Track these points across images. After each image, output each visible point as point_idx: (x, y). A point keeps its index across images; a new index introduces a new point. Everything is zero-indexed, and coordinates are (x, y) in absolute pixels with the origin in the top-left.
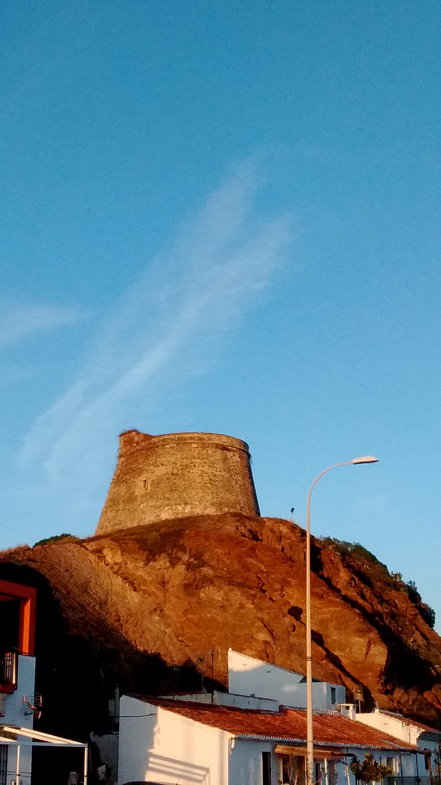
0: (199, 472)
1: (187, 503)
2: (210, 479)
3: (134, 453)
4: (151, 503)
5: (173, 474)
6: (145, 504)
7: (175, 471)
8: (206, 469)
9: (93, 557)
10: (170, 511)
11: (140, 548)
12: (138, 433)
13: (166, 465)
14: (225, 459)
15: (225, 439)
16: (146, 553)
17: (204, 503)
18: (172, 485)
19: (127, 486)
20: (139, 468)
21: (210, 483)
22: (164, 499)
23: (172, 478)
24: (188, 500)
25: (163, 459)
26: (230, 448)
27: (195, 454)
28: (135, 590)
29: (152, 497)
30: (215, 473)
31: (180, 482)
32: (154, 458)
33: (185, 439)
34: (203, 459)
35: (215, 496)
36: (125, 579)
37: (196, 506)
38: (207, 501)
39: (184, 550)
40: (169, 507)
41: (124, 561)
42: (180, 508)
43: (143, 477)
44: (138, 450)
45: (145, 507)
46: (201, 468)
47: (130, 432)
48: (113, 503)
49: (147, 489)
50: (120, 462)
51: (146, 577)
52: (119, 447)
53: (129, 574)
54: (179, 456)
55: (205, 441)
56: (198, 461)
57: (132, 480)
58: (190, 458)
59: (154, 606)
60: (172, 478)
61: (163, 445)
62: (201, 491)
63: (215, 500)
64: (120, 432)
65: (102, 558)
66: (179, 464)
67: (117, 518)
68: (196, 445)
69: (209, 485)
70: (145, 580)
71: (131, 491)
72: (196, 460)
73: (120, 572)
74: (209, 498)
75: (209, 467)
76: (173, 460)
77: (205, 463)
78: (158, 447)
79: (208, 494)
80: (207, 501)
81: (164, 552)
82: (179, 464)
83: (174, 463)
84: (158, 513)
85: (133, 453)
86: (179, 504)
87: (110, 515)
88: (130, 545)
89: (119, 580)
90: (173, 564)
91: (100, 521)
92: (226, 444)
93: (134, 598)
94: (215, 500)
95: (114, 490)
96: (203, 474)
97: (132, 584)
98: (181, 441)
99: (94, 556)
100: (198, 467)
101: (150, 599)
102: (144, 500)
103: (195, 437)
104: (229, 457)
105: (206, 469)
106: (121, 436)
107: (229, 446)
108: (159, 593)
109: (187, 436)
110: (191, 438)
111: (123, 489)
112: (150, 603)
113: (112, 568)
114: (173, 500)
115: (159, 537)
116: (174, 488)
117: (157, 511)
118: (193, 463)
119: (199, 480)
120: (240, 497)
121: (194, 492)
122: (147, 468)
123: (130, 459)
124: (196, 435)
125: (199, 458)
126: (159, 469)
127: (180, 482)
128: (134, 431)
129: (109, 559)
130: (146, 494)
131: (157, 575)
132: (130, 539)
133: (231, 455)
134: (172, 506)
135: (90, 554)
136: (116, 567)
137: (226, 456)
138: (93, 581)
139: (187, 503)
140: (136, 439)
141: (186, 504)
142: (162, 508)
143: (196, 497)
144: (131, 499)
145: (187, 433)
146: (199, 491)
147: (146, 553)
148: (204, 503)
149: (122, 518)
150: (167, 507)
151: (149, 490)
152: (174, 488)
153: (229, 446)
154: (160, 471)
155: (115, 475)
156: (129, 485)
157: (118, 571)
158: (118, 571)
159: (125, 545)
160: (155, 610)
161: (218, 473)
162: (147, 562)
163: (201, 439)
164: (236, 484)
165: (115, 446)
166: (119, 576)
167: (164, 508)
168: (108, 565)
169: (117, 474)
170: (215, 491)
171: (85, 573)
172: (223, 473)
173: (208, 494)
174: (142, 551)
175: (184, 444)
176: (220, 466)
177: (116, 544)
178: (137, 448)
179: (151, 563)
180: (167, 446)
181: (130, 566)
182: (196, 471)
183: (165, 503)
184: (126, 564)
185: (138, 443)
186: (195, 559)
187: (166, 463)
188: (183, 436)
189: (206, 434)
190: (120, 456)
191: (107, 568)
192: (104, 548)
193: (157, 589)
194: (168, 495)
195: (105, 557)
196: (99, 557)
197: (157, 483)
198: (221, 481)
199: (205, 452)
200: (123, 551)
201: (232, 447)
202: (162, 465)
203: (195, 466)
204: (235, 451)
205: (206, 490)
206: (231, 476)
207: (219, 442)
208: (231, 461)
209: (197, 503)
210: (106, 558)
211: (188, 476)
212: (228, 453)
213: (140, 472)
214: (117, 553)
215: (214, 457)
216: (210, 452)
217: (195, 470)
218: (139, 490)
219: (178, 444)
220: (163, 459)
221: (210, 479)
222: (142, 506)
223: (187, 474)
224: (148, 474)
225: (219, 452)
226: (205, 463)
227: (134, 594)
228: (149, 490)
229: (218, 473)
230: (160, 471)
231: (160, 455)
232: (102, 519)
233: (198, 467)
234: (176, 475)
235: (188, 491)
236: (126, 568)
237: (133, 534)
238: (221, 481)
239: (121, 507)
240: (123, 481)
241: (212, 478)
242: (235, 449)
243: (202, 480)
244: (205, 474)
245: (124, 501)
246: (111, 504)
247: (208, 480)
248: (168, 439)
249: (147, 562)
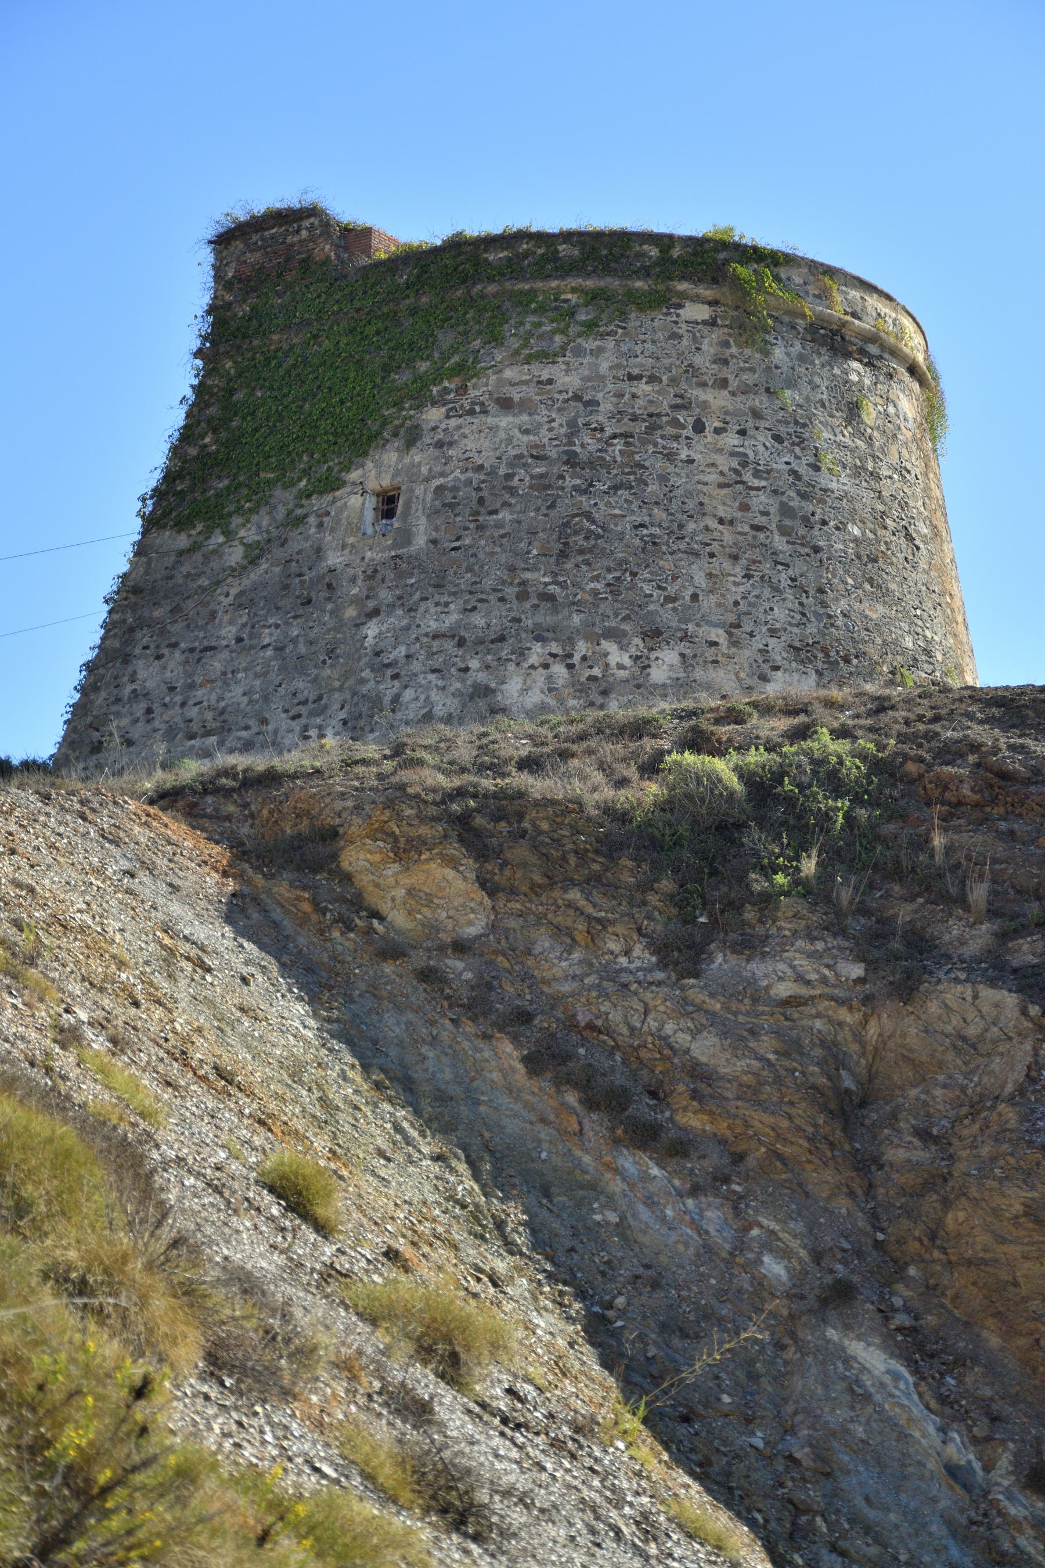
0: (725, 463)
2: (786, 511)
5: (571, 460)
6: (397, 619)
7: (588, 444)
8: (759, 445)
10: (559, 670)
13: (526, 406)
17: (757, 643)
21: (784, 531)
22: (522, 596)
23: (569, 482)
24: (667, 617)
27: (698, 360)
34: (745, 390)
37: (710, 653)
38: (773, 632)
40: (555, 648)
43: (380, 469)
46: (731, 440)
49: (405, 537)
51: (706, 1048)
54: (604, 367)
56: (717, 400)
58: (674, 381)
60: (569, 482)
66: (607, 406)
69: (779, 542)
70: (700, 1074)
74: (780, 615)
75: (778, 438)
79: (776, 589)
82: (607, 406)
83: (577, 397)
84: (482, 677)
86: (611, 634)
94: (812, 629)
96: (748, 476)
100: (718, 431)
105: (759, 445)
117: (474, 664)
118: (686, 407)
119: (722, 504)
125: (723, 383)
126: (492, 421)
134: (571, 641)
139: (657, 633)
141: (654, 635)
143: (707, 602)
146: (727, 565)
148: (757, 643)
149: (236, 694)
150: (537, 648)
151: (420, 541)
154: (486, 439)
165: (185, 295)
167: (522, 653)
173: (776, 589)
182: (709, 456)
187: (530, 391)
197: (473, 503)
202: (506, 404)
203: (699, 427)
205: (767, 567)
209: (718, 635)
211: (663, 478)
217: (698, 451)
221: (786, 511)
222: (372, 630)
223: (659, 465)
226: (757, 414)
228: (420, 541)
230: (486, 439)
233: (718, 431)
234: (591, 464)
235: (666, 564)
239: (228, 632)
241: (796, 503)
243: (745, 507)
244: (757, 474)
245: (244, 602)
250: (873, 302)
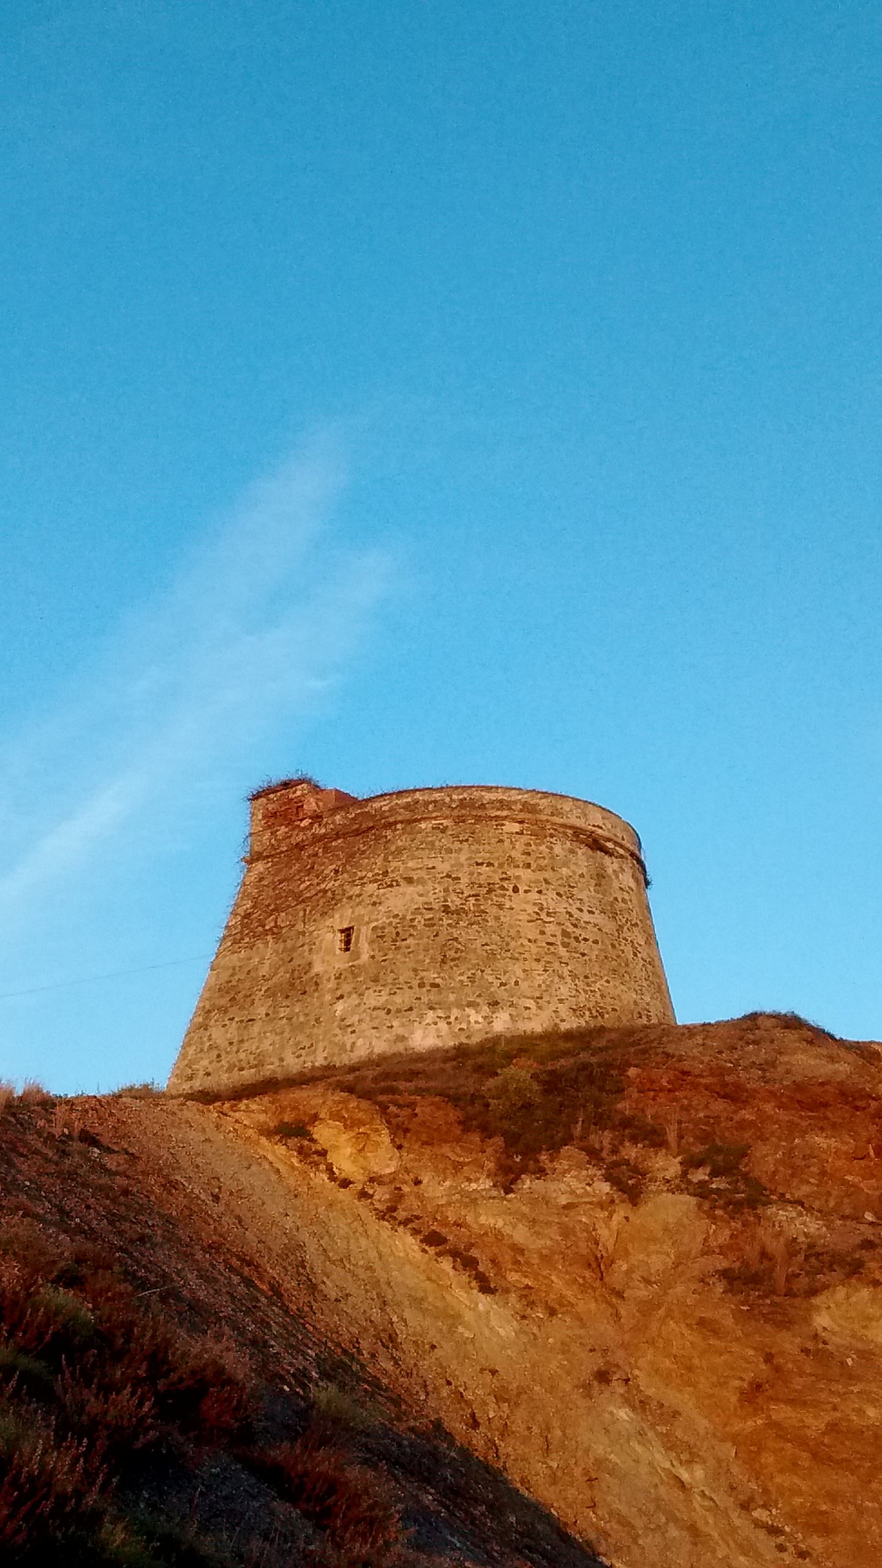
0: (531, 909)
1: (497, 1003)
2: (565, 934)
3: (302, 848)
4: (372, 999)
5: (446, 909)
6: (354, 1000)
7: (454, 901)
8: (550, 899)
9: (278, 1152)
10: (442, 1025)
11: (465, 1125)
12: (316, 789)
13: (421, 881)
14: (600, 877)
15: (596, 818)
16: (499, 1141)
18: (449, 940)
19: (281, 946)
20: (325, 891)
21: (565, 945)
22: (421, 985)
23: (446, 922)
24: (502, 994)
25: (410, 864)
26: (610, 845)
27: (513, 854)
28: (486, 1288)
29: (376, 980)
30: (576, 914)
31: (470, 935)
32: (379, 861)
33: (483, 806)
34: (541, 869)
35: (581, 984)
36: (433, 1239)
37: (526, 1013)
38: (561, 1001)
39: (655, 1139)
40: (440, 1013)
41: (407, 1171)
42: (474, 1016)
43: (340, 919)
44: (317, 839)
45: (353, 1013)
46: (534, 896)
47: (286, 785)
48: (226, 998)
50: (253, 877)
51: (520, 1234)
52: (247, 830)
53: (445, 1223)
54: (463, 858)
55: (544, 818)
56: (525, 874)
57: (300, 927)
58: (501, 865)
59: (590, 1363)
60: (446, 922)
61: (409, 822)
62: (540, 967)
63: (582, 998)
64: (257, 783)
65: (314, 1156)
66: (465, 880)
67: (246, 1045)
68: (516, 827)
69: (562, 951)
71: (295, 962)
72: (520, 872)
73: (401, 1214)
74: (564, 991)
75: (558, 894)
76: (444, 867)
77: (547, 882)
78: (390, 825)
79: (561, 977)
80: (561, 1001)
81: (568, 1140)
82: (465, 880)
83: (448, 876)
84: (401, 1031)
85: (300, 847)
86: (470, 1004)
87: (218, 1035)
88: (424, 1110)
89: (407, 1244)
90: (630, 1186)
91: (183, 1055)
92: (600, 831)
93: (490, 1324)
94: (582, 998)
95: (234, 959)
96: (543, 916)
97: (466, 1262)
98: (470, 810)
99: (281, 1149)
100: (526, 892)
101: (560, 1329)
102: (346, 988)
103: (515, 802)
104: (610, 871)
105: (550, 899)
106: (256, 797)
107: (609, 840)
108: (587, 1305)
109: (488, 796)
110: (502, 804)
111: (266, 956)
112: (564, 1348)
113: (363, 1195)
114: (453, 990)
115: (536, 1087)
116: (451, 954)
120: (648, 999)
121: (517, 969)
122: (357, 890)
123: (288, 865)
124: (515, 796)
125: (529, 866)
126: (404, 890)
127: (470, 935)
128: (301, 781)
129: (344, 1160)
130: (354, 971)
131: (566, 1232)
132: (419, 1091)
133: (616, 866)
134: (449, 1009)
135: (263, 1140)
136: (381, 1194)
137: (603, 867)
138: (312, 1247)
139: (497, 1003)
140: (311, 805)
141: (494, 1004)
142: (413, 1015)
143: (524, 985)
144: (298, 985)
145: (489, 789)
146: (534, 965)
147: (499, 1141)
149: (266, 1045)
150: (431, 1013)
151: (365, 957)
152: (451, 954)
153: (609, 840)
154: (401, 900)
155: (234, 914)
156: (289, 943)
157: (393, 1209)
158: (393, 1209)
159: (406, 1112)
160: (603, 1377)
161: (586, 917)
162: (507, 1179)
163: (528, 808)
164: (635, 955)
165: (234, 827)
166: (401, 1229)
167: (422, 1016)
168: (345, 1183)
169: (241, 911)
170: (580, 970)
171: (274, 1210)
172: (598, 918)
173: (561, 977)
174: (476, 1138)
175: (478, 819)
176: (587, 894)
177: (365, 1104)
178: (308, 840)
179: (527, 1183)
180: (423, 825)
181: (437, 1189)
182: (522, 905)
183: (425, 999)
184: (418, 1182)
185: (317, 818)
186: (714, 1174)
187: (423, 874)
188: (476, 794)
189: (546, 795)
190: (253, 858)
191: (344, 1195)
192: (315, 1118)
193: (584, 1287)
194: (432, 976)
195: (323, 1153)
196: (301, 1151)
198: (596, 942)
199: (543, 848)
200: (400, 1132)
201: (616, 843)
202: (409, 880)
203: (516, 890)
204: (622, 856)
206: (620, 928)
207: (580, 823)
208: (616, 884)
209: (530, 1003)
210: (330, 1158)
211: (497, 918)
212: (607, 860)
213: (331, 901)
214: (374, 1137)
215: (573, 867)
216: (558, 849)
218: (326, 956)
219: (460, 820)
220: (410, 864)
221: (565, 934)
222: (340, 1007)
223: (494, 911)
224: (360, 910)
225: (582, 851)
226: (547, 882)
227: (484, 1302)
228: (365, 957)
229: (586, 917)
230: (401, 900)
231: (399, 851)
232: (191, 1051)
233: (526, 892)
234: (457, 912)
235: (500, 964)
236: (420, 1197)
237: (414, 1074)
238: (596, 942)
239: (262, 1011)
240: (266, 933)
241: (571, 929)
242: (621, 851)
243: (543, 933)
244: (548, 914)
245: (270, 993)
246: (224, 1001)
247: (559, 933)
248: (427, 804)
249: (507, 1179)
250: (418, 795)
